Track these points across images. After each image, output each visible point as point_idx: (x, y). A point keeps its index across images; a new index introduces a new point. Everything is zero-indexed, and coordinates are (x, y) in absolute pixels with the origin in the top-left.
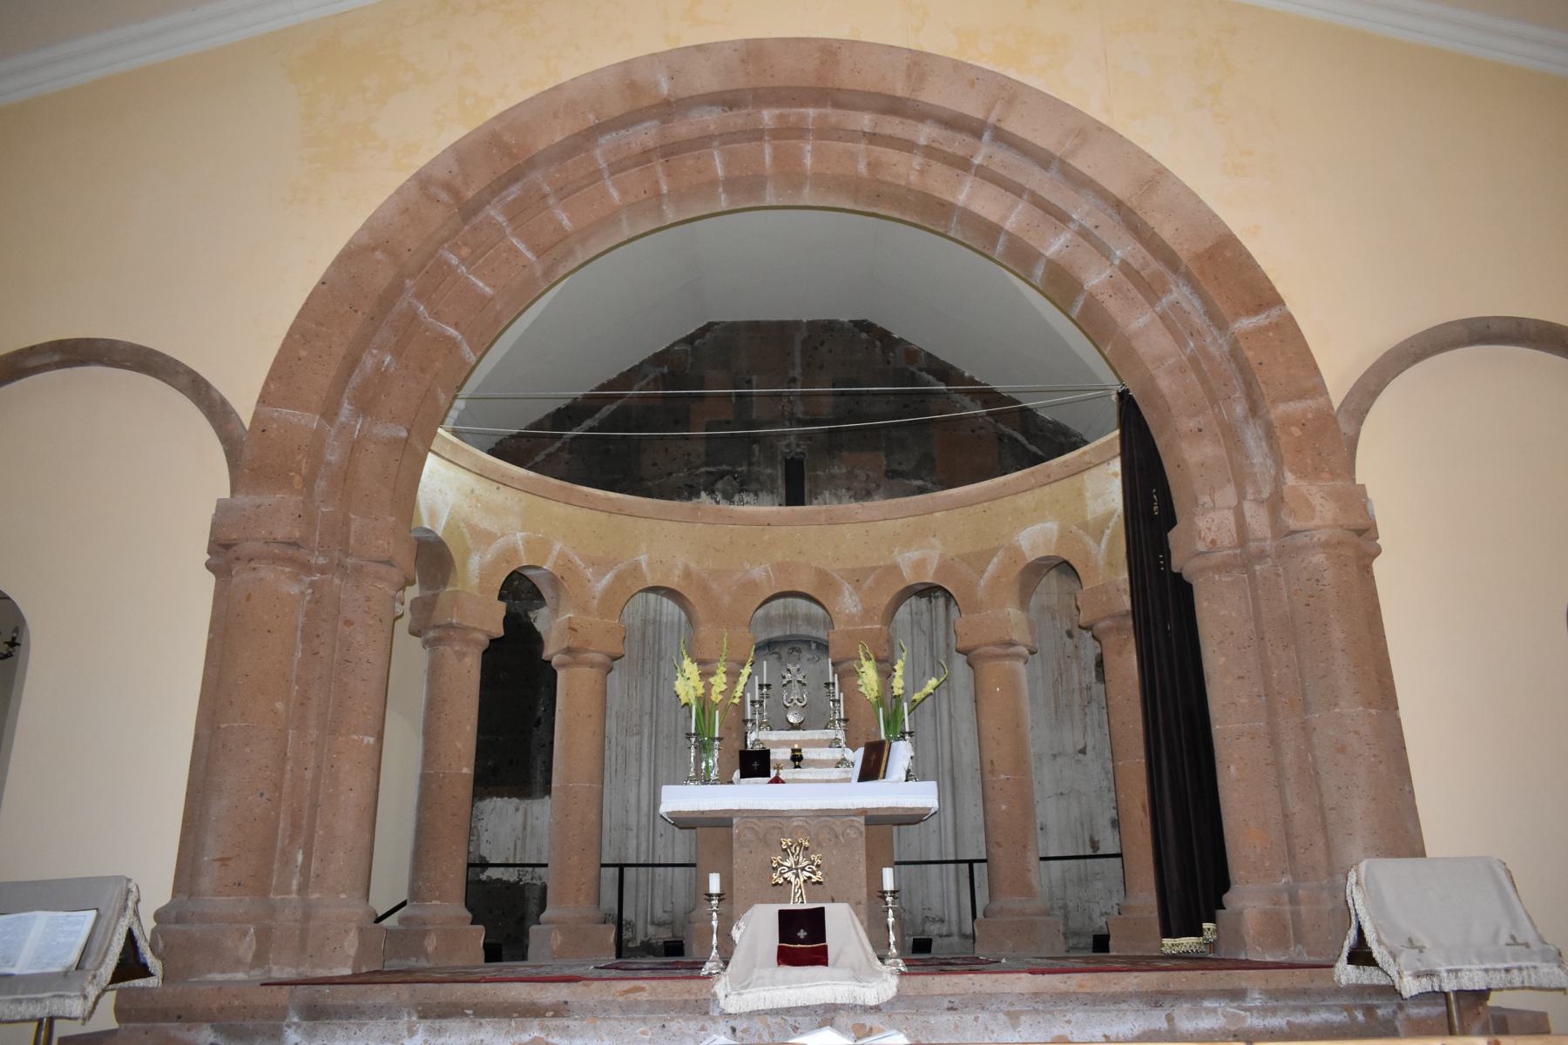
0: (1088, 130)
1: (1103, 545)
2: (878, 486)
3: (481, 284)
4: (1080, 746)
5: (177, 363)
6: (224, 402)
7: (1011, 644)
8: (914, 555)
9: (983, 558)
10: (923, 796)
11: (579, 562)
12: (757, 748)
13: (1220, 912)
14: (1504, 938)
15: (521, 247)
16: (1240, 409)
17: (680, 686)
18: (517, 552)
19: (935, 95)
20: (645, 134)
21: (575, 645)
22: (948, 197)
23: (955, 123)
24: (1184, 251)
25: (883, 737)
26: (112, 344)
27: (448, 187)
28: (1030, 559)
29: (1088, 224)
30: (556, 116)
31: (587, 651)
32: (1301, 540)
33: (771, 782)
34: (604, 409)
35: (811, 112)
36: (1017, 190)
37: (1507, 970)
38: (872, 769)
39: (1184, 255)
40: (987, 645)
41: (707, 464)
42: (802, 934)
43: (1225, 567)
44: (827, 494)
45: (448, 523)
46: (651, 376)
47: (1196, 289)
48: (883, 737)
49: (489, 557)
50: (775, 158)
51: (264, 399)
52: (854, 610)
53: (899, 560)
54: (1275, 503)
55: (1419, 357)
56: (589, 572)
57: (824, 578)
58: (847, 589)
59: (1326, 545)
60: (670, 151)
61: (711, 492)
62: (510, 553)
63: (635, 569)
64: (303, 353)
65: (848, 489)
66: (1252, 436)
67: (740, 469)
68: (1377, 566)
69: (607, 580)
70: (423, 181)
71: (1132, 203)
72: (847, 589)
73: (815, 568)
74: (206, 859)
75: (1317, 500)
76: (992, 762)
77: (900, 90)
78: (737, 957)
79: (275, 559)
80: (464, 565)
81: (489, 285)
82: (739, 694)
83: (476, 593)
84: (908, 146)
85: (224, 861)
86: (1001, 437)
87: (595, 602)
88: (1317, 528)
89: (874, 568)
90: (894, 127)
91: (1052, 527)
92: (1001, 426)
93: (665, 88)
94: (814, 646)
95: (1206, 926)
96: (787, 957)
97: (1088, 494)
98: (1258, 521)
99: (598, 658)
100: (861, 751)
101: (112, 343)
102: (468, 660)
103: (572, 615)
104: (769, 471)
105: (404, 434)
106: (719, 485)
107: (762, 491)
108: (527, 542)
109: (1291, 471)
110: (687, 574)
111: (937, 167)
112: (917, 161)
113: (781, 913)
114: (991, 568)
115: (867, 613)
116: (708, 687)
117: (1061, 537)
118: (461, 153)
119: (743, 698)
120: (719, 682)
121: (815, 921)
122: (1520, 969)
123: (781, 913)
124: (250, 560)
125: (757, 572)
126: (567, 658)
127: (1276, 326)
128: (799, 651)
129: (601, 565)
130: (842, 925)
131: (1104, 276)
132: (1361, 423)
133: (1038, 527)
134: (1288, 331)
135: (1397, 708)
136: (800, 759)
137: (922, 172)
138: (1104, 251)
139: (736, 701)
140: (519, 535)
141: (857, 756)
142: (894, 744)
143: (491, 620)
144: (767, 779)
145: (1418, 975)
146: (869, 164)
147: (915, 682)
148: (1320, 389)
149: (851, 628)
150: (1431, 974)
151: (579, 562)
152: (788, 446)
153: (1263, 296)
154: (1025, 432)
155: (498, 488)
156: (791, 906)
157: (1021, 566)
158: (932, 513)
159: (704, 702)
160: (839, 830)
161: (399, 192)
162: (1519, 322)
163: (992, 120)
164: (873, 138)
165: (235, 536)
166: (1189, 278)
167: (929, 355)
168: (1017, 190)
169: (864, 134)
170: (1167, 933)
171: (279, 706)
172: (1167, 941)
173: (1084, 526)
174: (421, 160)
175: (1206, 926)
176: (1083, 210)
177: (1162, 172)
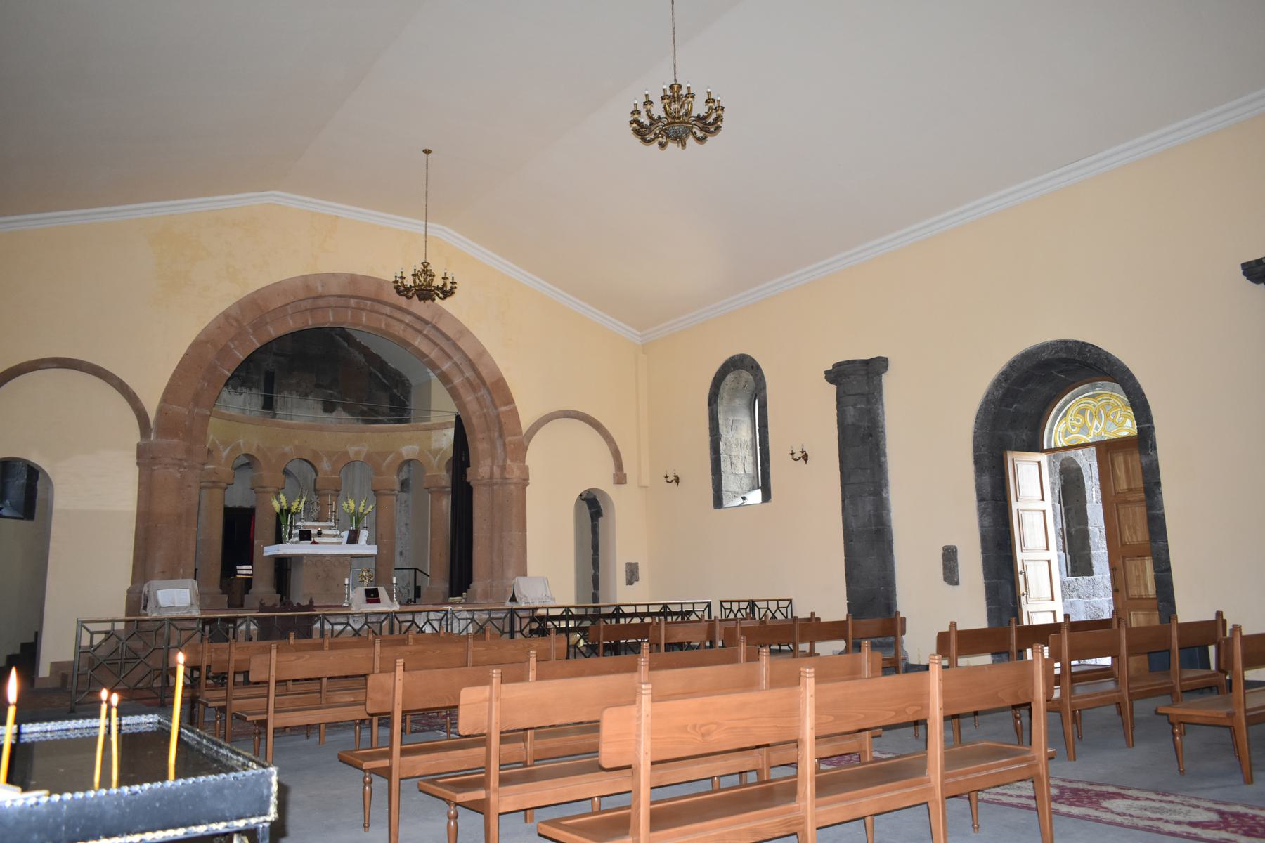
0: (464, 332)
1: (436, 460)
2: (311, 392)
3: (238, 354)
5: (112, 374)
7: (394, 490)
8: (356, 449)
10: (373, 550)
13: (468, 590)
15: (254, 340)
16: (496, 434)
20: (308, 304)
24: (488, 381)
27: (237, 320)
29: (459, 363)
30: (278, 295)
31: (221, 482)
32: (509, 481)
36: (436, 344)
39: (488, 383)
40: (385, 490)
43: (485, 485)
44: (286, 392)
47: (490, 393)
50: (352, 316)
51: (165, 399)
52: (327, 469)
53: (349, 450)
54: (503, 468)
58: (325, 459)
59: (515, 484)
63: (238, 445)
64: (180, 383)
65: (297, 392)
66: (499, 444)
68: (527, 488)
69: (228, 449)
70: (226, 315)
71: (475, 361)
72: (325, 459)
74: (156, 572)
75: (515, 470)
76: (381, 535)
79: (174, 464)
84: (401, 321)
86: (371, 374)
87: (223, 460)
89: (338, 452)
91: (417, 448)
92: (371, 368)
95: (464, 594)
96: (369, 601)
97: (433, 439)
98: (497, 471)
99: (224, 485)
104: (257, 377)
110: (258, 449)
111: (409, 330)
112: (402, 326)
114: (389, 459)
121: (376, 592)
124: (166, 465)
125: (287, 449)
130: (382, 592)
131: (461, 379)
132: (530, 441)
133: (411, 447)
134: (514, 413)
136: (321, 534)
138: (462, 372)
141: (346, 534)
144: (310, 542)
146: (386, 324)
148: (521, 432)
149: (326, 476)
150: (528, 603)
152: (268, 365)
153: (509, 400)
154: (383, 374)
161: (216, 319)
162: (578, 412)
163: (433, 322)
166: (488, 390)
168: (436, 344)
172: (451, 598)
173: (430, 451)
176: (457, 358)
177: (485, 351)
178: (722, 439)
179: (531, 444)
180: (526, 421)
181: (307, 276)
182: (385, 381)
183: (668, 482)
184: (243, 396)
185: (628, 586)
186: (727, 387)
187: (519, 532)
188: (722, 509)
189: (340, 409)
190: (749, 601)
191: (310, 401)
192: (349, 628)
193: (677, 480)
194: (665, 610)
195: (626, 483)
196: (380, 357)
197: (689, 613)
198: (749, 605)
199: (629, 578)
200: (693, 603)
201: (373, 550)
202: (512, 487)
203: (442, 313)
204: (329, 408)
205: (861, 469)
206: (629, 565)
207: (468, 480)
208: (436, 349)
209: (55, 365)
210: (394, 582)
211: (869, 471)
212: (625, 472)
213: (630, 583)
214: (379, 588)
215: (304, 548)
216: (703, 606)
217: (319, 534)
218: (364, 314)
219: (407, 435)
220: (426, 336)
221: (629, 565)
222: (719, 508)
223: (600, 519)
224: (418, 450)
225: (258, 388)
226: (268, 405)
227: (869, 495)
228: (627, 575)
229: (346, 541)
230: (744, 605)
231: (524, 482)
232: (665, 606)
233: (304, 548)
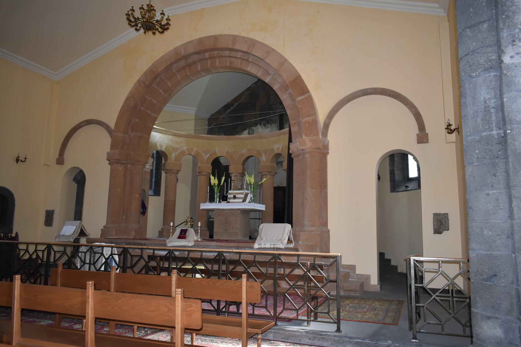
3: (154, 101)
8: (277, 146)
11: (201, 152)
20: (182, 63)
22: (246, 69)
33: (227, 203)
34: (235, 104)
35: (216, 52)
37: (274, 245)
45: (165, 147)
46: (246, 94)
52: (265, 160)
56: (203, 154)
57: (259, 153)
58: (263, 154)
60: (189, 65)
61: (260, 125)
63: (215, 152)
69: (207, 156)
70: (139, 81)
72: (263, 154)
81: (155, 101)
83: (174, 162)
87: (205, 161)
88: (307, 148)
90: (233, 54)
99: (205, 174)
105: (141, 135)
106: (262, 122)
107: (273, 123)
108: (187, 149)
109: (305, 135)
118: (146, 74)
122: (276, 244)
125: (244, 151)
127: (306, 98)
130: (191, 232)
134: (310, 100)
137: (241, 63)
140: (185, 148)
144: (227, 202)
145: (259, 245)
146: (230, 63)
151: (201, 152)
155: (179, 138)
158: (281, 135)
171: (119, 190)
177: (286, 60)
184: (268, 129)
187: (313, 189)
195: (427, 142)
205: (470, 27)
206: (435, 215)
210: (199, 225)
211: (486, 25)
212: (427, 132)
213: (438, 231)
217: (235, 197)
221: (435, 215)
225: (275, 123)
227: (486, 70)
228: (434, 224)
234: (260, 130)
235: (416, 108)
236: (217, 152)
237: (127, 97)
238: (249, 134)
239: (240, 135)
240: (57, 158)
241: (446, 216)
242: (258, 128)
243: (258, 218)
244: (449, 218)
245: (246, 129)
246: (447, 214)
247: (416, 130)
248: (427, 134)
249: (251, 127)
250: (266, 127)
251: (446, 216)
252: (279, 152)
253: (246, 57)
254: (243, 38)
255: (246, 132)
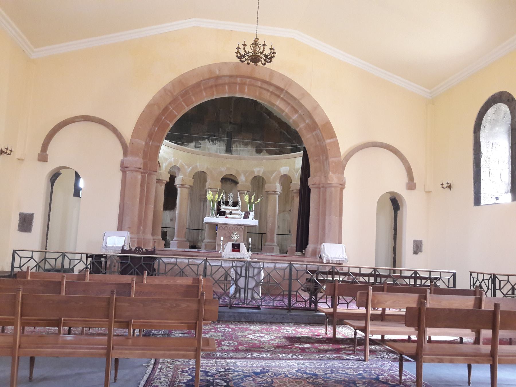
0: (305, 94)
3: (175, 112)
4: (290, 209)
6: (120, 134)
7: (276, 192)
8: (258, 169)
9: (273, 172)
10: (256, 223)
11: (184, 165)
12: (223, 210)
14: (341, 256)
15: (184, 104)
17: (208, 196)
18: (172, 162)
19: (275, 82)
21: (183, 183)
23: (278, 88)
25: (248, 211)
26: (95, 117)
27: (172, 93)
28: (283, 174)
29: (302, 114)
31: (186, 185)
35: (248, 80)
36: (289, 104)
38: (246, 217)
41: (207, 132)
42: (236, 247)
47: (321, 132)
48: (248, 211)
49: (167, 164)
51: (132, 136)
53: (254, 170)
55: (361, 149)
56: (186, 167)
61: (208, 139)
62: (170, 163)
64: (140, 127)
67: (216, 134)
68: (344, 190)
69: (190, 168)
70: (165, 89)
72: (242, 175)
73: (236, 170)
77: (268, 80)
78: (225, 250)
79: (136, 171)
80: (162, 166)
82: (220, 199)
84: (268, 90)
85: (129, 228)
87: (188, 174)
90: (265, 86)
93: (217, 72)
94: (230, 180)
95: (303, 251)
96: (233, 251)
99: (188, 186)
100: (244, 213)
101: (95, 117)
102: (162, 186)
103: (182, 177)
108: (174, 160)
109: (331, 172)
113: (233, 244)
114: (274, 175)
115: (246, 180)
116: (214, 197)
117: (289, 171)
118: (173, 83)
119: (221, 200)
120: (217, 197)
121: (238, 246)
123: (233, 244)
125: (223, 169)
126: (181, 186)
128: (227, 181)
129: (189, 166)
130: (243, 247)
131: (304, 125)
133: (285, 168)
134: (336, 144)
135: (342, 217)
138: (305, 121)
139: (219, 200)
142: (251, 212)
143: (166, 178)
144: (224, 217)
147: (256, 199)
148: (340, 156)
149: (242, 184)
151: (184, 165)
154: (287, 132)
156: (234, 243)
157: (280, 176)
159: (213, 200)
160: (239, 228)
161: (159, 91)
162: (382, 143)
163: (285, 89)
164: (261, 87)
165: (128, 166)
167: (266, 109)
168: (289, 104)
169: (259, 86)
170: (297, 252)
172: (296, 253)
173: (294, 169)
174: (164, 84)
175: (303, 251)
177: (318, 105)
178: (483, 157)
179: (348, 163)
180: (344, 149)
181: (210, 65)
182: (289, 136)
183: (443, 188)
185: (414, 255)
186: (489, 118)
188: (480, 206)
189: (264, 151)
190: (491, 274)
191: (249, 148)
192: (176, 267)
193: (450, 187)
194: (416, 275)
196: (287, 124)
197: (436, 278)
198: (491, 277)
199: (415, 250)
200: (440, 272)
201: (256, 223)
202: (333, 189)
203: (272, 73)
204: (259, 152)
207: (309, 185)
208: (289, 107)
209: (83, 120)
212: (415, 182)
213: (415, 253)
214: (240, 243)
215: (220, 220)
216: (449, 276)
217: (231, 213)
218: (247, 87)
219: (283, 161)
220: (282, 99)
222: (478, 206)
223: (398, 212)
224: (288, 170)
226: (229, 151)
229: (243, 217)
230: (487, 277)
231: (342, 186)
232: (416, 272)
233: (220, 220)
234: (207, 144)
235: (409, 164)
236: (198, 166)
237: (149, 103)
238: (196, 147)
239: (186, 146)
240: (39, 153)
241: (421, 242)
242: (205, 142)
243: (201, 229)
244: (423, 244)
245: (191, 141)
246: (422, 241)
247: (405, 179)
248: (415, 183)
249: (198, 141)
250: (213, 143)
251: (421, 242)
252: (260, 175)
253: (278, 93)
254: (281, 75)
255: (193, 144)
